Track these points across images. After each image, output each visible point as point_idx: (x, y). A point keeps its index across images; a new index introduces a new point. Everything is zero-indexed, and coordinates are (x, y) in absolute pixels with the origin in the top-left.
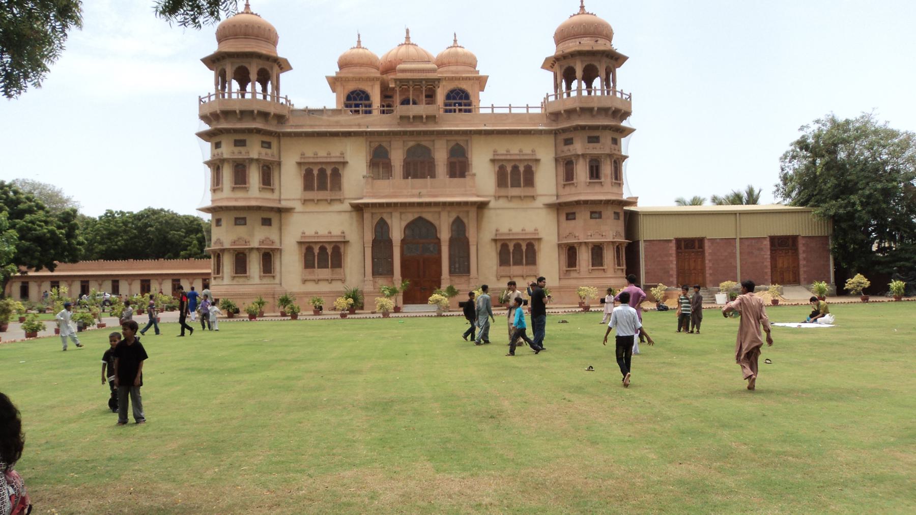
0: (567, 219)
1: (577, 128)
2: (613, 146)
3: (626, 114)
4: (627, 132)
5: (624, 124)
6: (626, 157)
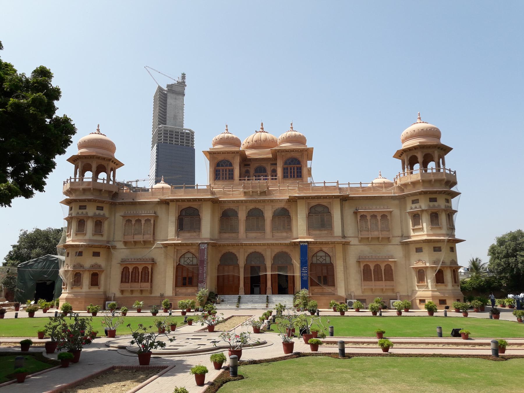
0: (416, 252)
1: (421, 193)
2: (447, 204)
3: (455, 183)
4: (455, 194)
5: (453, 189)
6: (456, 211)
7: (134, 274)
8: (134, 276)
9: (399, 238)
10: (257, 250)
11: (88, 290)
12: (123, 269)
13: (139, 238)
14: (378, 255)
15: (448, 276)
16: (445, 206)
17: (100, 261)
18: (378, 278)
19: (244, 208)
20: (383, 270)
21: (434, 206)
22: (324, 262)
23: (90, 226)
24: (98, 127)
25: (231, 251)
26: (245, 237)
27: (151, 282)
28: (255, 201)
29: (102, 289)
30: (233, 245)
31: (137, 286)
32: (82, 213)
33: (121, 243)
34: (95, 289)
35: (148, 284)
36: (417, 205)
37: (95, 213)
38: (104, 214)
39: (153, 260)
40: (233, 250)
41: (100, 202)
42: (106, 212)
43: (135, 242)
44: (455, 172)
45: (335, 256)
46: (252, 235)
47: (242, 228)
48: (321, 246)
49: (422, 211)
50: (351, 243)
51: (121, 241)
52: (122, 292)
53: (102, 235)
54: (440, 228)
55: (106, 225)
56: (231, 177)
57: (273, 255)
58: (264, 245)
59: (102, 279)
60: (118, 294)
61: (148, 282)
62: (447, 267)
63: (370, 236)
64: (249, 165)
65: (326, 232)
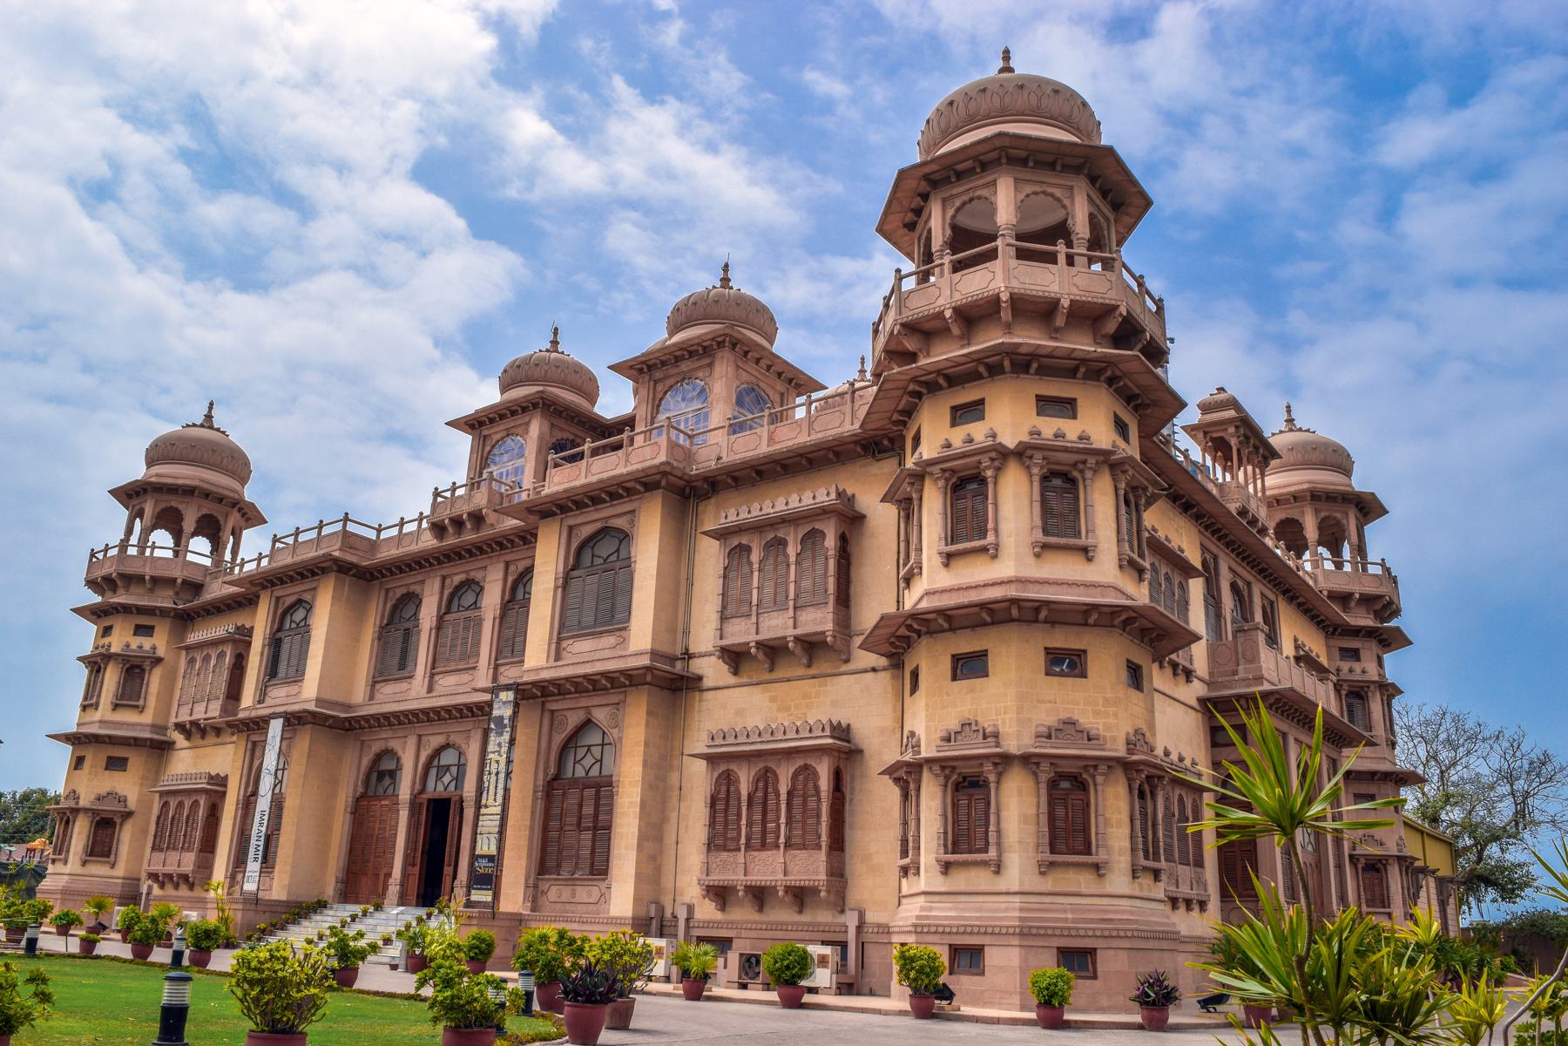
11: (78, 869)
15: (1017, 808)
17: (128, 786)
22: (594, 772)
24: (211, 408)
29: (120, 870)
34: (98, 869)
41: (141, 610)
42: (159, 642)
45: (620, 739)
48: (584, 702)
50: (708, 682)
53: (141, 709)
55: (155, 680)
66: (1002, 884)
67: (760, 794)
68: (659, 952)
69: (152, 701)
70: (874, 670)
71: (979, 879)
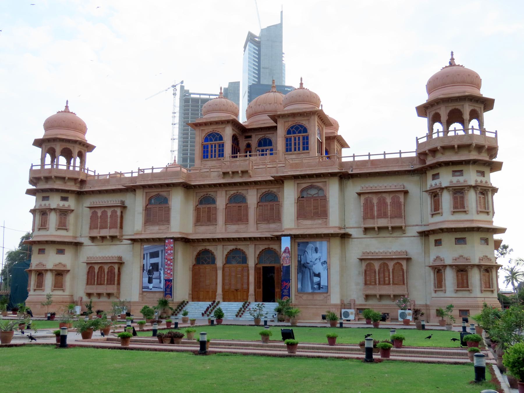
0: (435, 246)
7: (99, 274)
8: (99, 277)
9: (417, 227)
10: (239, 247)
12: (89, 269)
13: (105, 232)
14: (390, 251)
16: (476, 181)
17: (66, 260)
18: (384, 282)
19: (224, 193)
20: (391, 271)
21: (458, 181)
23: (53, 219)
24: (67, 103)
25: (208, 248)
26: (224, 230)
27: (119, 284)
28: (235, 184)
29: (67, 292)
30: (208, 240)
31: (102, 289)
32: (45, 205)
33: (87, 239)
35: (115, 287)
36: (437, 181)
37: (58, 205)
38: (69, 206)
39: (120, 258)
40: (211, 248)
42: (71, 203)
43: (103, 238)
44: (496, 133)
46: (233, 228)
47: (221, 217)
49: (442, 189)
50: (353, 236)
51: (86, 237)
52: (89, 295)
54: (465, 212)
55: (71, 218)
56: (221, 155)
57: (258, 253)
58: (245, 239)
59: (67, 279)
60: (85, 299)
61: (114, 284)
62: (473, 266)
63: (376, 226)
64: (250, 137)
65: (320, 221)
66: (472, 295)
67: (382, 269)
68: (352, 313)
69: (71, 227)
70: (414, 236)
71: (466, 294)
